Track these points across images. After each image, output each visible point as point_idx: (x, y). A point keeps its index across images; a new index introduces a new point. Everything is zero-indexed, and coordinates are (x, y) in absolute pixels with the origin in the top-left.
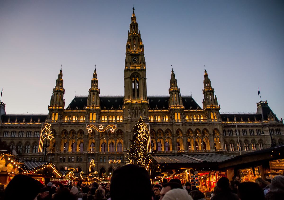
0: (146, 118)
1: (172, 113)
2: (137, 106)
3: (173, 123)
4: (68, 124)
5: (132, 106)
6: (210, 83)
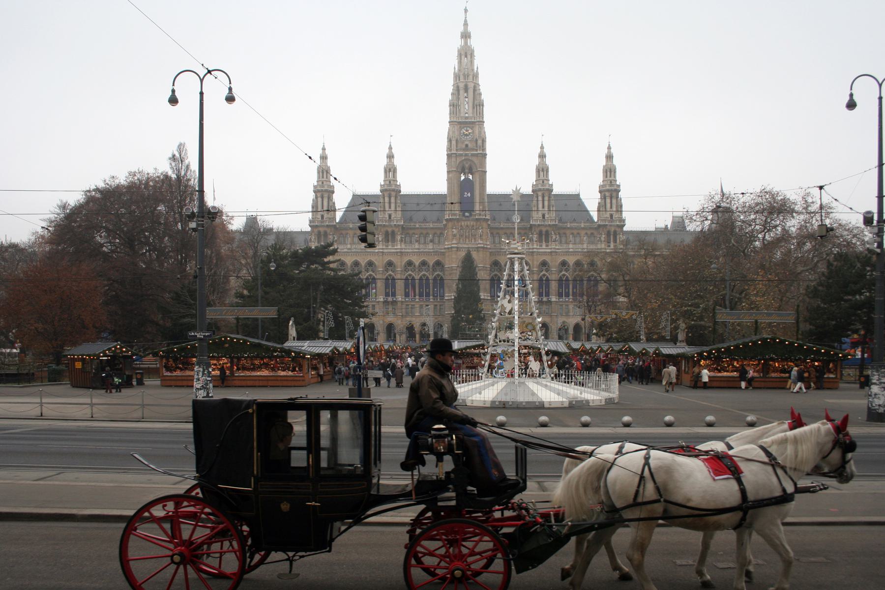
0: (482, 246)
1: (533, 230)
2: (469, 223)
3: (535, 250)
4: (346, 250)
5: (460, 224)
6: (615, 172)
